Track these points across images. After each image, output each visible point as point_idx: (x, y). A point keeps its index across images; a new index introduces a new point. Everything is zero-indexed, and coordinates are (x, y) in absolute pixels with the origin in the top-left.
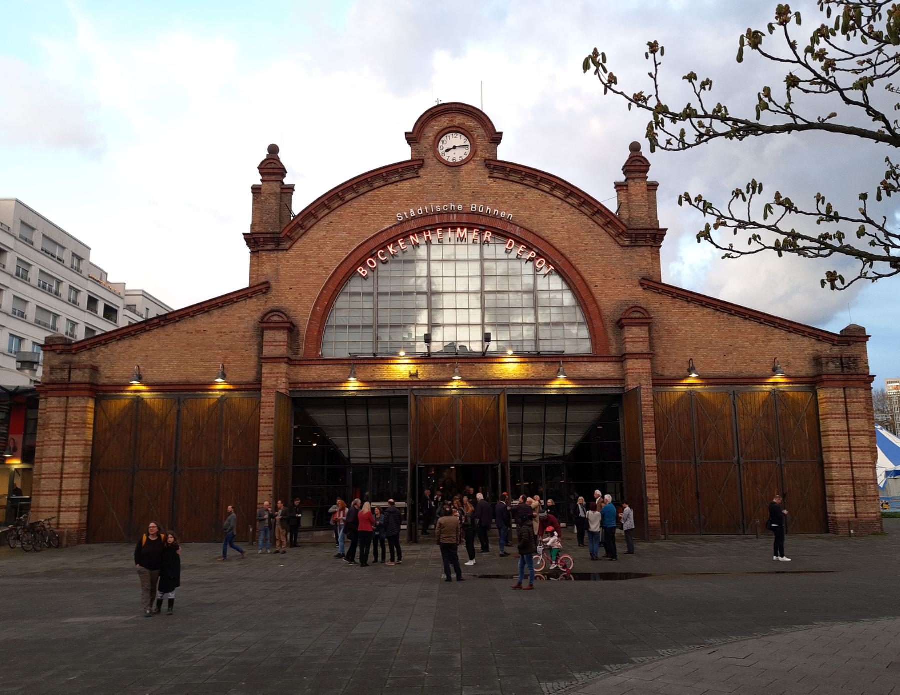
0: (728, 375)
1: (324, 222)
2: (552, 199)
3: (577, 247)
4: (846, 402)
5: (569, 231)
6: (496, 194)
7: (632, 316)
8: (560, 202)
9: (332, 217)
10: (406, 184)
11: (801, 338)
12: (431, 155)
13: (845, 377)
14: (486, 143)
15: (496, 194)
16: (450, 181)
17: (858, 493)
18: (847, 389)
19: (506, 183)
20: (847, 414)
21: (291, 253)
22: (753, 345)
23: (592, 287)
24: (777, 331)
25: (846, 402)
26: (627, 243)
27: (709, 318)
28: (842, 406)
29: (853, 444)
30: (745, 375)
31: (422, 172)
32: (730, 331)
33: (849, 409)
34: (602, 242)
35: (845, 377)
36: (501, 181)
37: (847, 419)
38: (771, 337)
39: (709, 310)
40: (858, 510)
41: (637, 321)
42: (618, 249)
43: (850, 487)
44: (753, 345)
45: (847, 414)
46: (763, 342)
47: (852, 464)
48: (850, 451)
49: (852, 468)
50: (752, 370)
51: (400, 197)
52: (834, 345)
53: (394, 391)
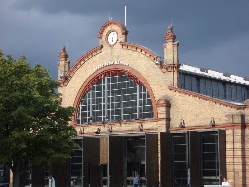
0: (197, 125)
1: (76, 74)
2: (141, 55)
3: (149, 74)
4: (233, 136)
5: (146, 68)
6: (124, 55)
7: (160, 103)
8: (144, 56)
9: (78, 72)
10: (98, 56)
11: (225, 107)
12: (105, 43)
13: (232, 125)
14: (121, 35)
15: (124, 55)
16: (110, 52)
17: (236, 176)
18: (234, 130)
19: (127, 50)
20: (233, 141)
21: (67, 86)
22: (207, 111)
23: (153, 90)
24: (216, 104)
25: (233, 136)
26: (165, 71)
27: (192, 101)
28: (232, 138)
29: (235, 154)
30: (203, 125)
31: (102, 50)
32: (199, 106)
33: (234, 139)
34: (157, 71)
35: (232, 125)
36: (126, 50)
37: (233, 143)
38: (213, 107)
39: (192, 97)
40: (235, 183)
41: (161, 105)
42: (162, 74)
43: (233, 173)
44: (207, 111)
45: (233, 141)
46: (211, 110)
47: (234, 163)
48: (234, 157)
49: (234, 164)
50: (206, 122)
51: (96, 61)
52: (237, 110)
53: (94, 136)
